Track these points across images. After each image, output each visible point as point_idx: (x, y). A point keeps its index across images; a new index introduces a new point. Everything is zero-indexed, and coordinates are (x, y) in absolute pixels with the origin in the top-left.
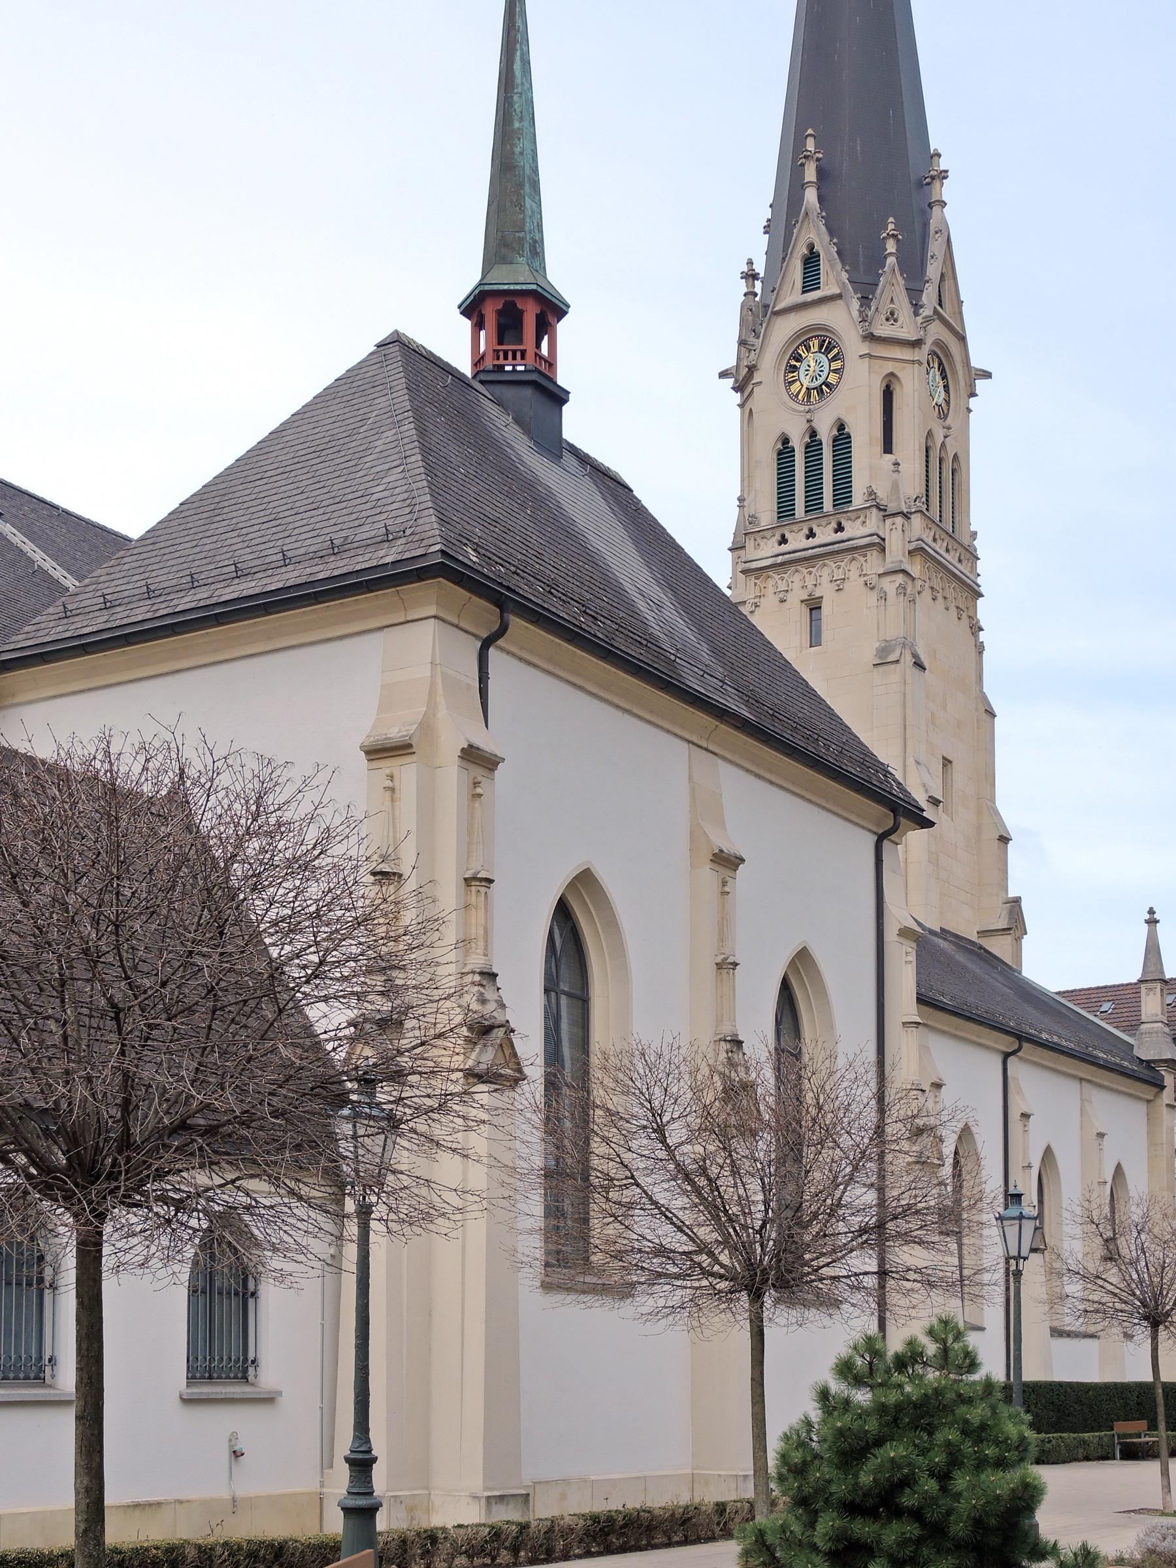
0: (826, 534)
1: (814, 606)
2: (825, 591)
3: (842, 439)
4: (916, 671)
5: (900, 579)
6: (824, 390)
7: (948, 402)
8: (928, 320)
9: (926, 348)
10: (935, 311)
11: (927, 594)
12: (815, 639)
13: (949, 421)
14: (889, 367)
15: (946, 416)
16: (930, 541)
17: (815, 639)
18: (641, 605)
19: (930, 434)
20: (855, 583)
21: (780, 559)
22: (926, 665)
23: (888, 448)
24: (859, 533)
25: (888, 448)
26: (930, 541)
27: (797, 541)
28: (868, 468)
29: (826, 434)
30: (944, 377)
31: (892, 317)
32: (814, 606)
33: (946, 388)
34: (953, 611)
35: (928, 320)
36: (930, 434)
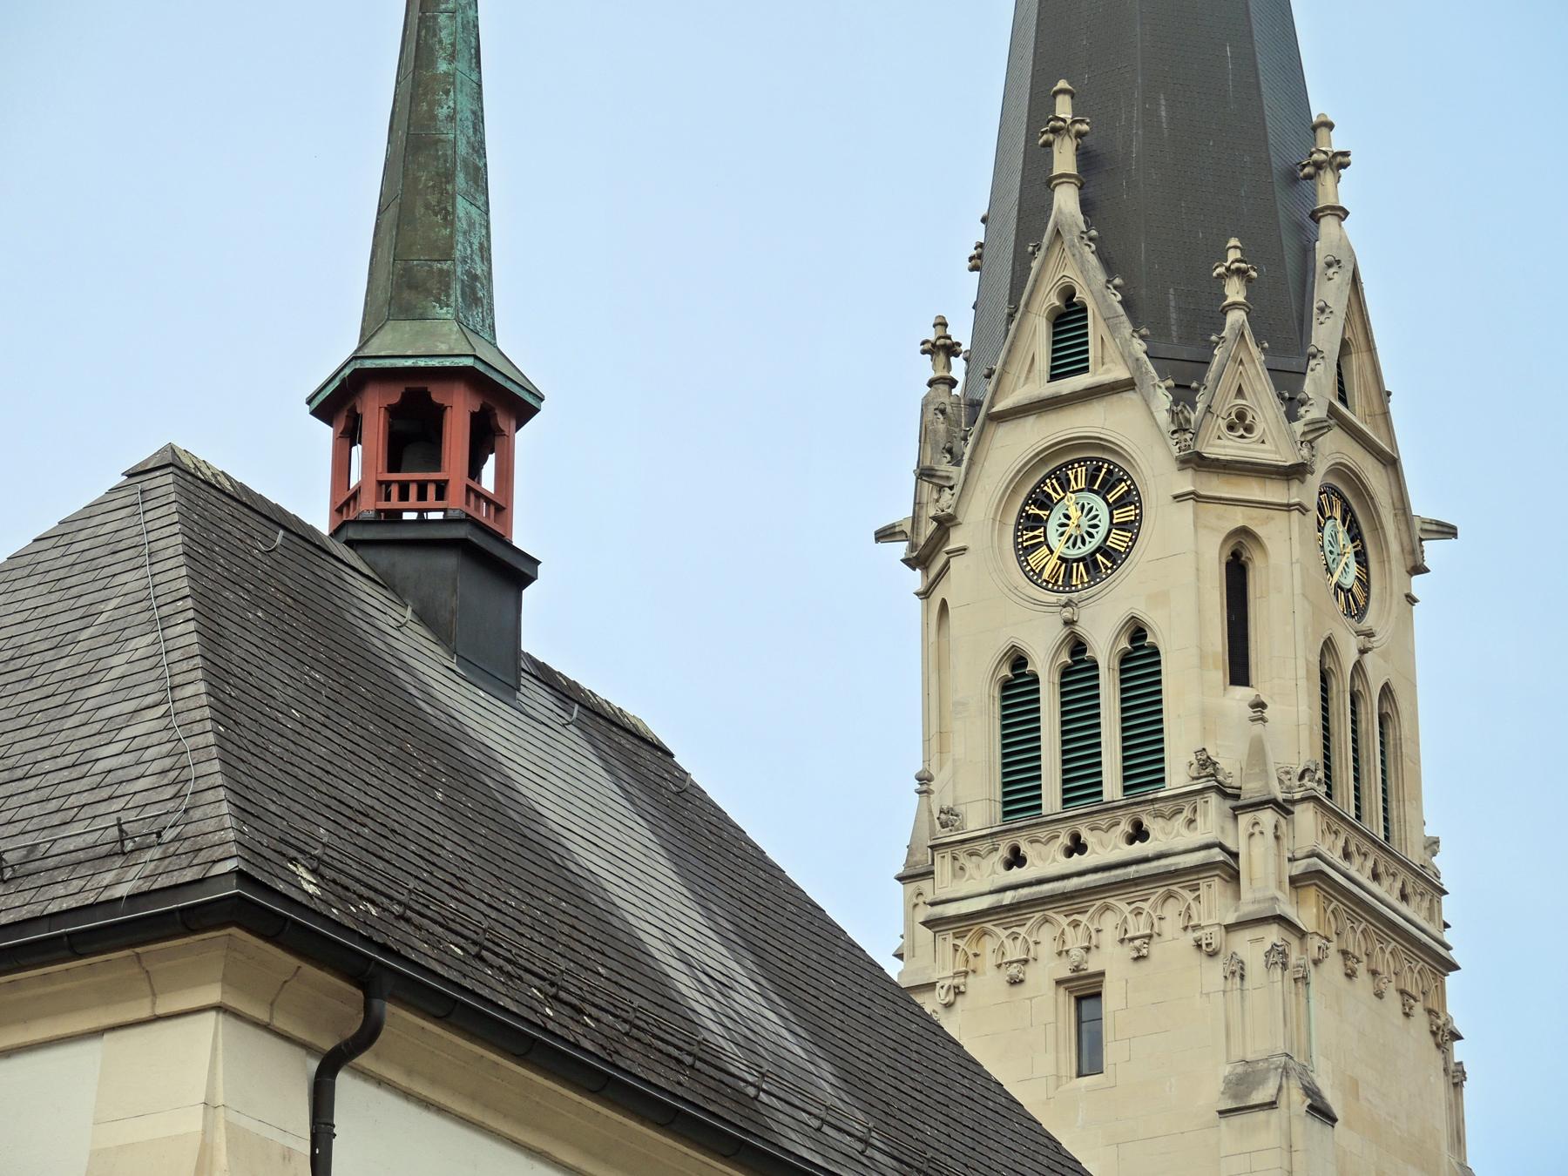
0: (1106, 846)
1: (1085, 992)
2: (1110, 959)
3: (1140, 656)
4: (1316, 1125)
5: (1273, 934)
6: (1100, 562)
7: (1365, 584)
8: (1317, 428)
9: (1315, 481)
10: (1332, 411)
11: (1334, 965)
12: (1089, 1059)
13: (1370, 621)
14: (1238, 518)
15: (1361, 613)
16: (1336, 857)
17: (1089, 1059)
18: (683, 983)
19: (1328, 646)
20: (1174, 944)
21: (1008, 898)
22: (1337, 1110)
23: (1239, 672)
24: (1180, 844)
25: (1239, 672)
26: (1336, 857)
27: (1046, 860)
28: (1198, 712)
29: (1105, 647)
30: (1355, 535)
31: (1240, 423)
32: (1085, 992)
33: (1361, 557)
34: (1393, 1001)
35: (1317, 428)
36: (1328, 646)
